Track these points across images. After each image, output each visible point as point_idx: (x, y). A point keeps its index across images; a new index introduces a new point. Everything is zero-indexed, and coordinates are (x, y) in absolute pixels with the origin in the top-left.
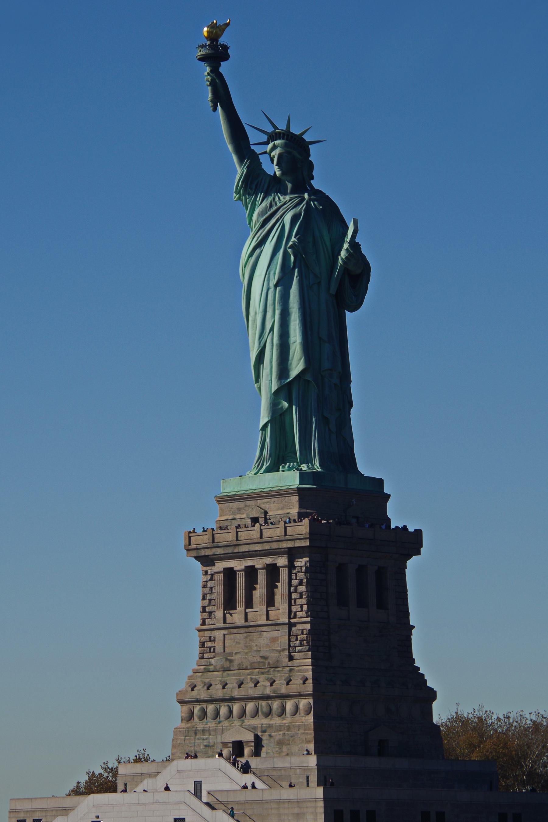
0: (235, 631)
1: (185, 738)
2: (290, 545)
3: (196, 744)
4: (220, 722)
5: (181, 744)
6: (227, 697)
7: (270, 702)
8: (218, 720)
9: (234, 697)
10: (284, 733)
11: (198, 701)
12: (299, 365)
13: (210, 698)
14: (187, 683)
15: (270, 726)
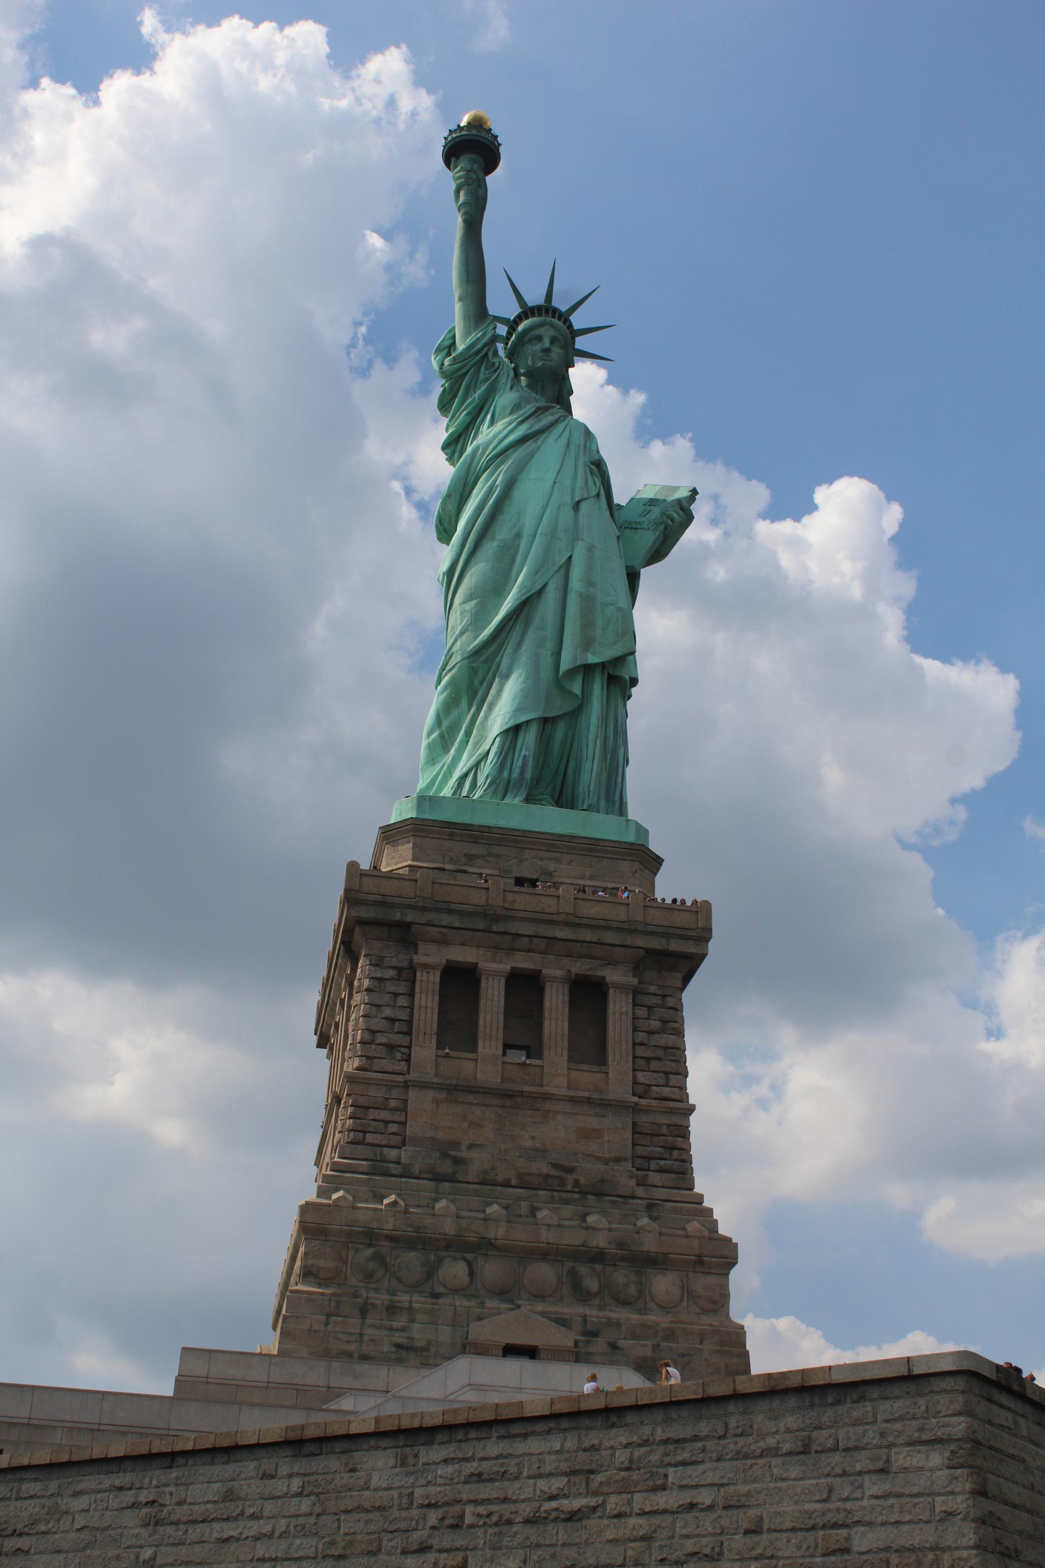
0: (471, 1098)
1: (327, 1319)
2: (655, 944)
3: (366, 1338)
4: (436, 1296)
5: (316, 1331)
6: (472, 1238)
7: (598, 1267)
8: (428, 1290)
9: (494, 1241)
10: (659, 1345)
11: (370, 1236)
12: (620, 643)
13: (415, 1234)
14: (322, 1192)
15: (610, 1323)
